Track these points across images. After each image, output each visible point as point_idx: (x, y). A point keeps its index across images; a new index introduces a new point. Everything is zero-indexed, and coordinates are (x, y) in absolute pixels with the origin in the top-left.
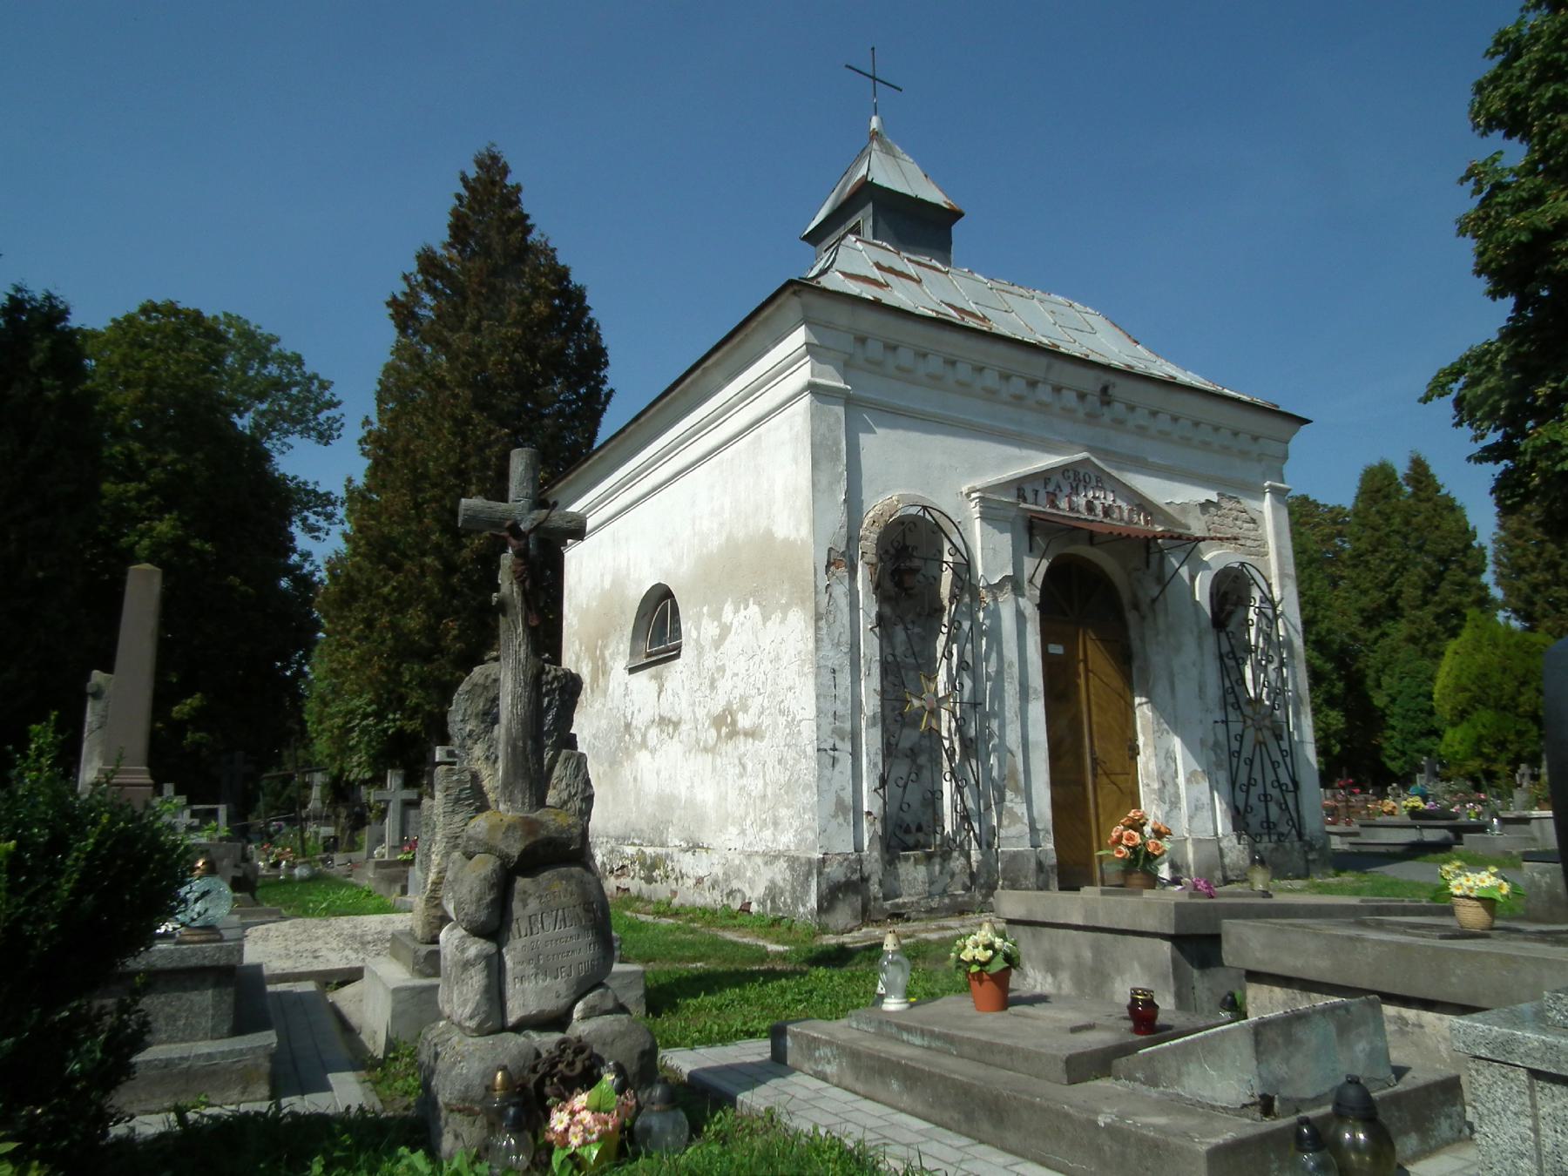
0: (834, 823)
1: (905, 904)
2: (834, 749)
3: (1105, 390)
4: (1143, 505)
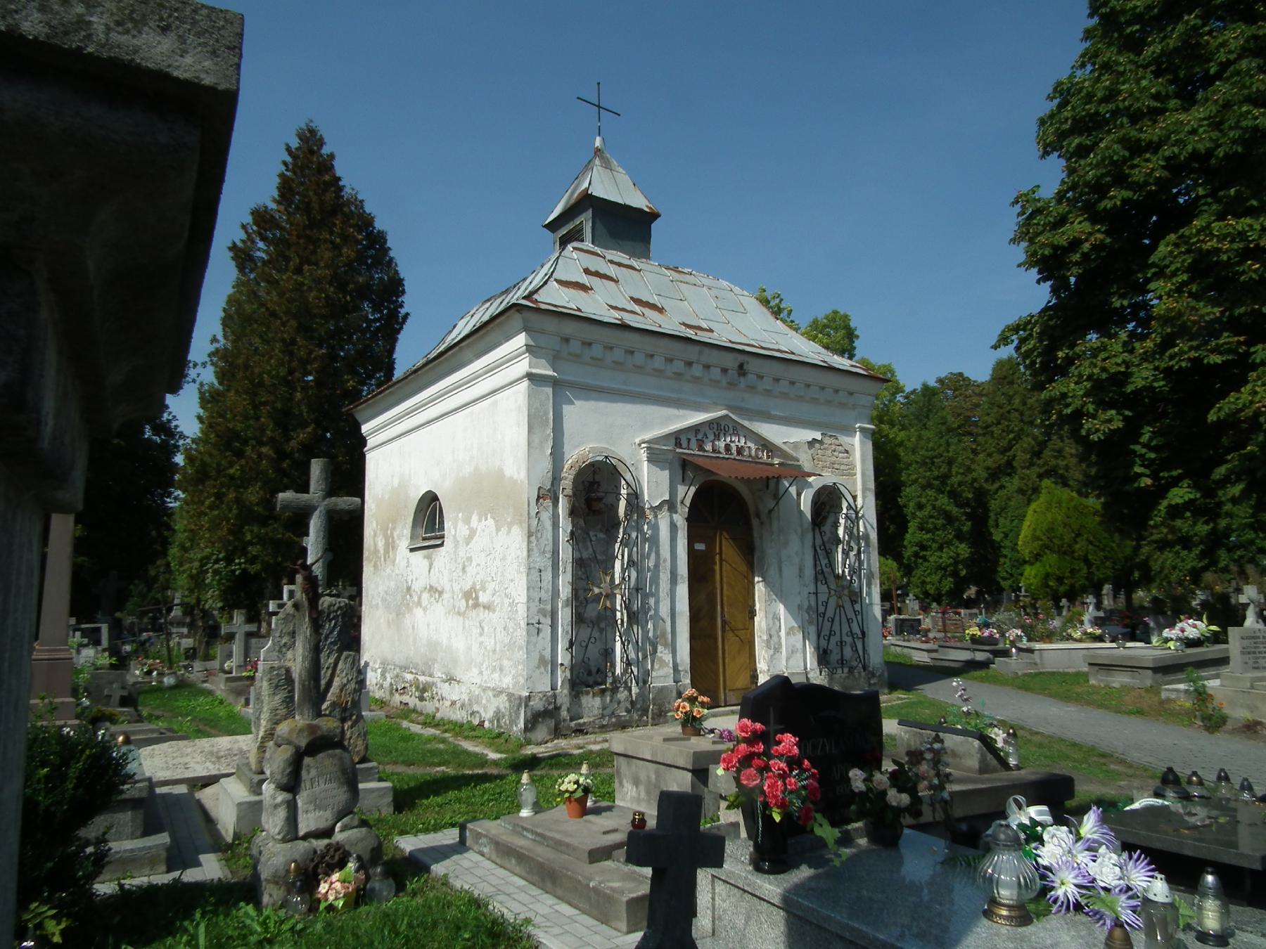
0: (538, 672)
1: (585, 723)
2: (539, 623)
3: (741, 366)
4: (766, 445)
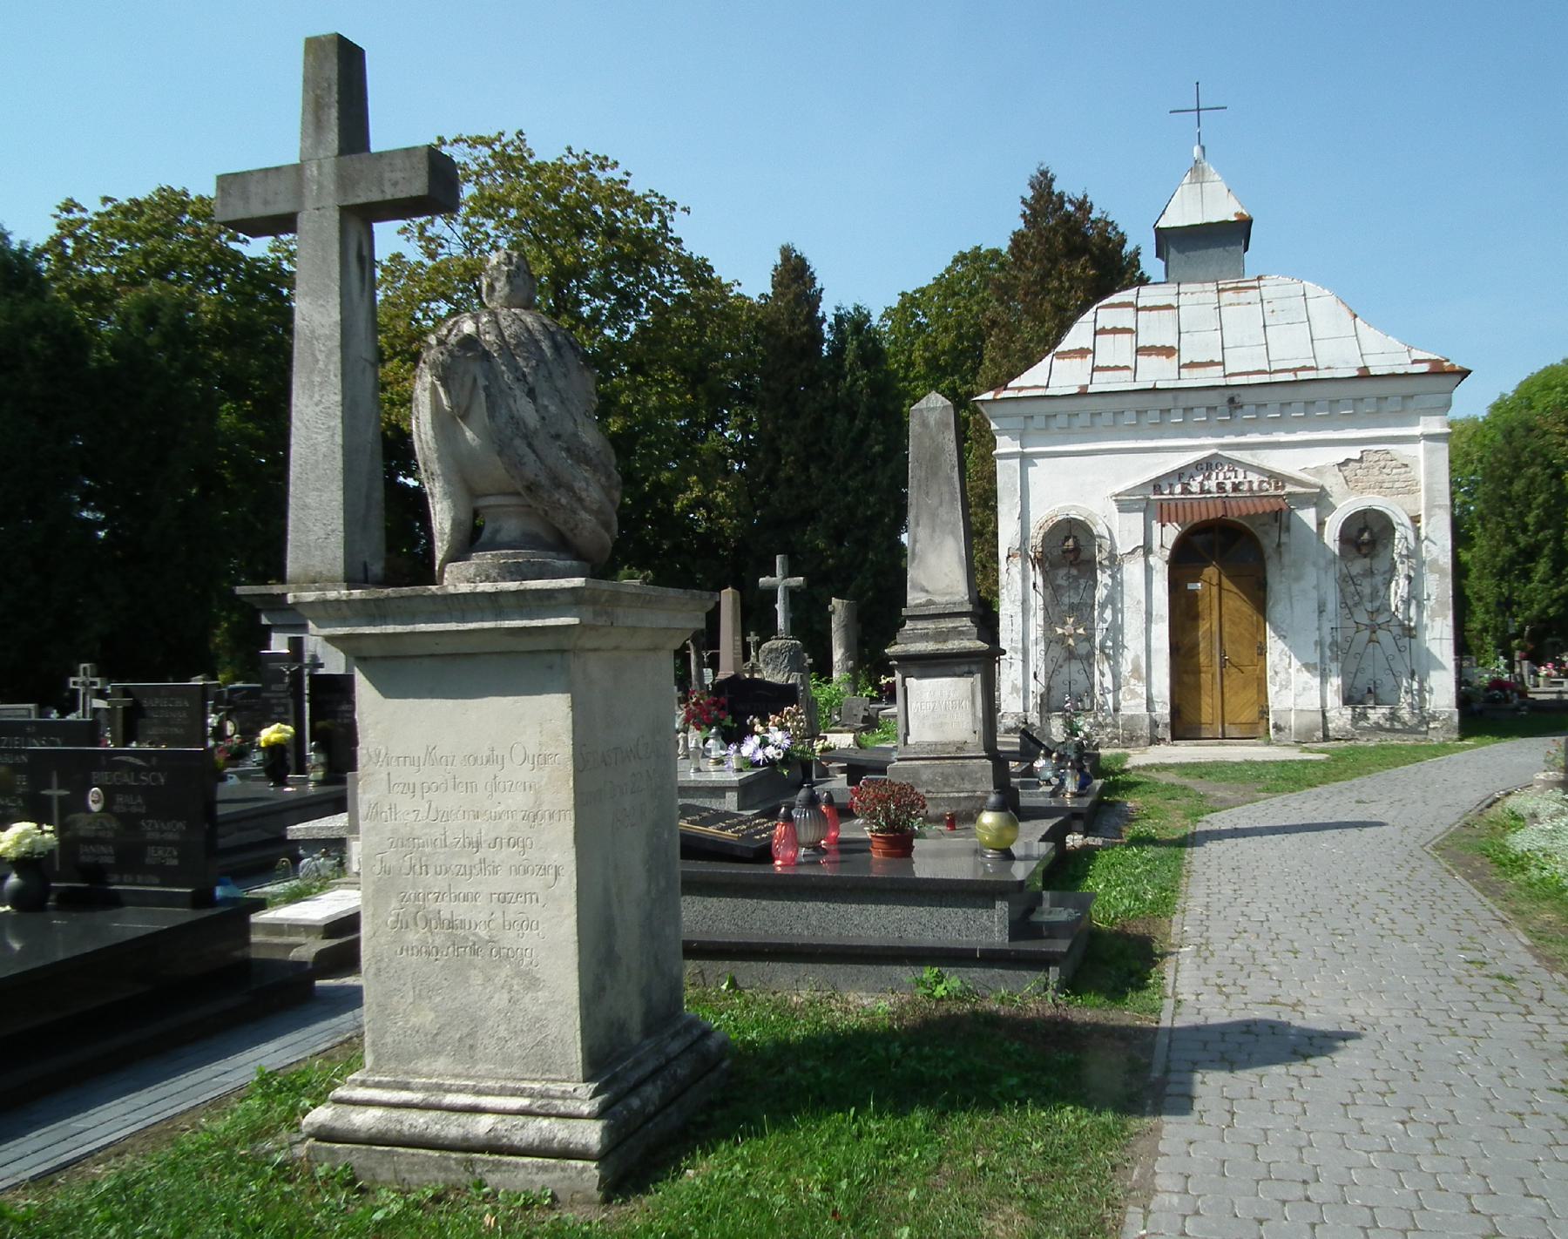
3: (1231, 400)
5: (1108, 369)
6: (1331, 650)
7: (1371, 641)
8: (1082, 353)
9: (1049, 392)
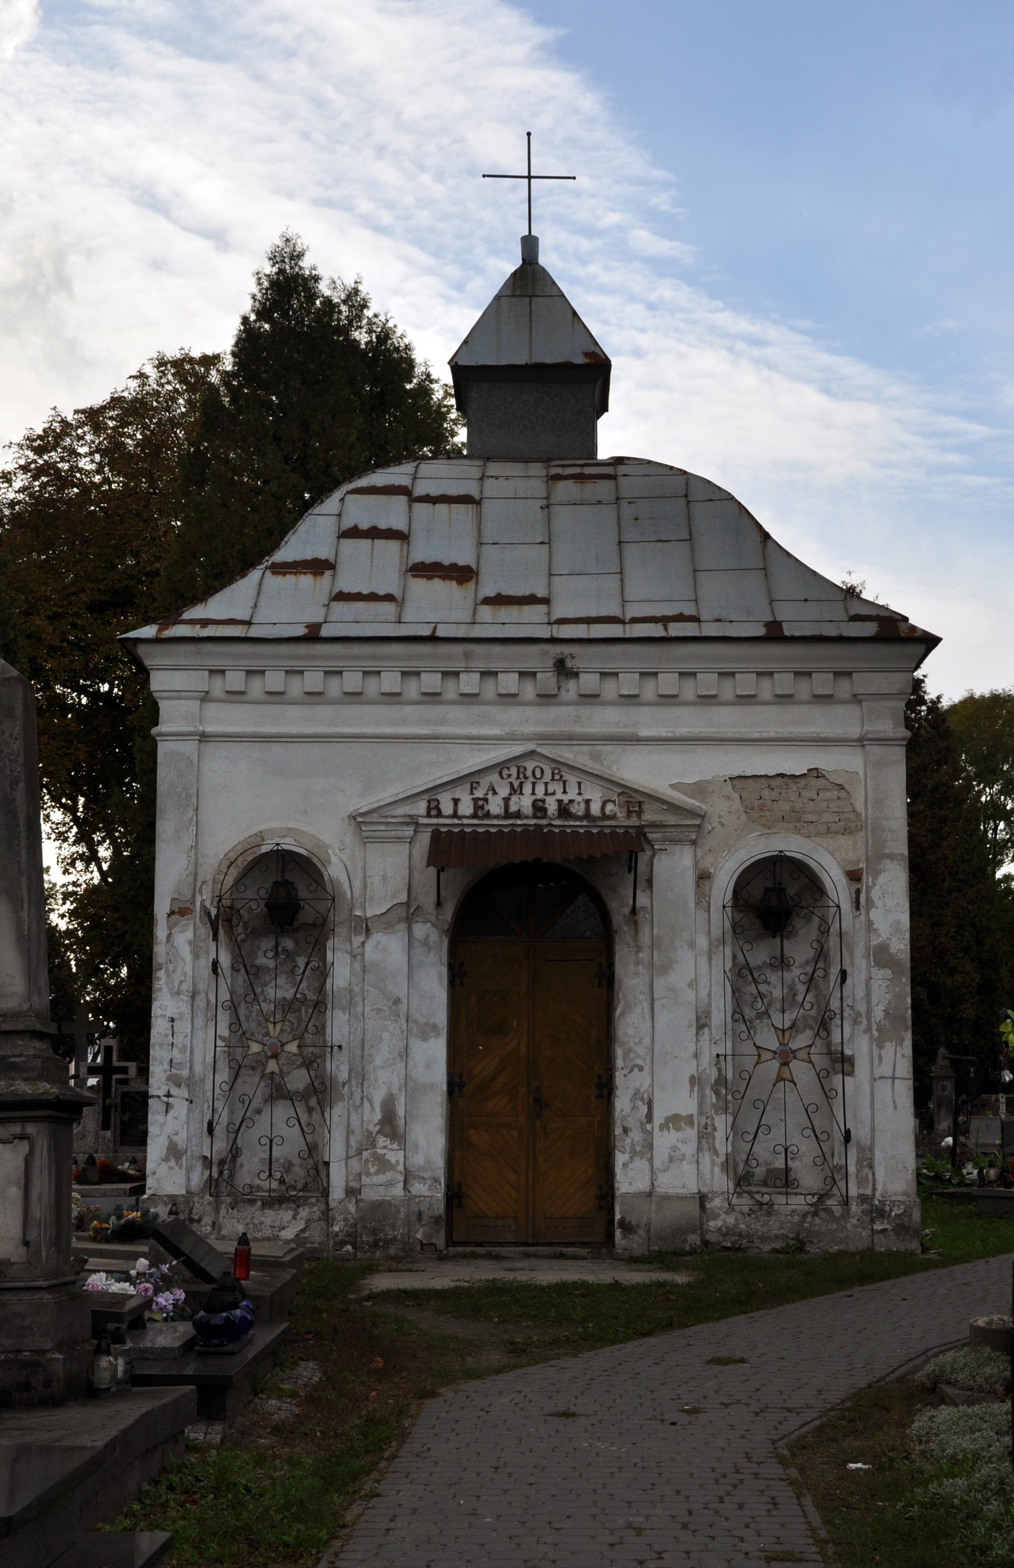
0: (165, 1166)
2: (169, 1095)
5: (358, 597)
6: (717, 1093)
7: (780, 1078)
8: (317, 567)
9: (254, 632)
